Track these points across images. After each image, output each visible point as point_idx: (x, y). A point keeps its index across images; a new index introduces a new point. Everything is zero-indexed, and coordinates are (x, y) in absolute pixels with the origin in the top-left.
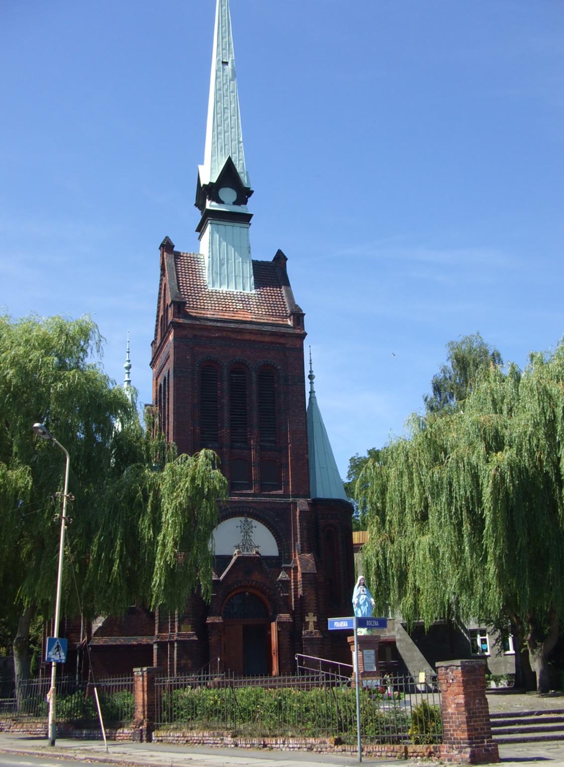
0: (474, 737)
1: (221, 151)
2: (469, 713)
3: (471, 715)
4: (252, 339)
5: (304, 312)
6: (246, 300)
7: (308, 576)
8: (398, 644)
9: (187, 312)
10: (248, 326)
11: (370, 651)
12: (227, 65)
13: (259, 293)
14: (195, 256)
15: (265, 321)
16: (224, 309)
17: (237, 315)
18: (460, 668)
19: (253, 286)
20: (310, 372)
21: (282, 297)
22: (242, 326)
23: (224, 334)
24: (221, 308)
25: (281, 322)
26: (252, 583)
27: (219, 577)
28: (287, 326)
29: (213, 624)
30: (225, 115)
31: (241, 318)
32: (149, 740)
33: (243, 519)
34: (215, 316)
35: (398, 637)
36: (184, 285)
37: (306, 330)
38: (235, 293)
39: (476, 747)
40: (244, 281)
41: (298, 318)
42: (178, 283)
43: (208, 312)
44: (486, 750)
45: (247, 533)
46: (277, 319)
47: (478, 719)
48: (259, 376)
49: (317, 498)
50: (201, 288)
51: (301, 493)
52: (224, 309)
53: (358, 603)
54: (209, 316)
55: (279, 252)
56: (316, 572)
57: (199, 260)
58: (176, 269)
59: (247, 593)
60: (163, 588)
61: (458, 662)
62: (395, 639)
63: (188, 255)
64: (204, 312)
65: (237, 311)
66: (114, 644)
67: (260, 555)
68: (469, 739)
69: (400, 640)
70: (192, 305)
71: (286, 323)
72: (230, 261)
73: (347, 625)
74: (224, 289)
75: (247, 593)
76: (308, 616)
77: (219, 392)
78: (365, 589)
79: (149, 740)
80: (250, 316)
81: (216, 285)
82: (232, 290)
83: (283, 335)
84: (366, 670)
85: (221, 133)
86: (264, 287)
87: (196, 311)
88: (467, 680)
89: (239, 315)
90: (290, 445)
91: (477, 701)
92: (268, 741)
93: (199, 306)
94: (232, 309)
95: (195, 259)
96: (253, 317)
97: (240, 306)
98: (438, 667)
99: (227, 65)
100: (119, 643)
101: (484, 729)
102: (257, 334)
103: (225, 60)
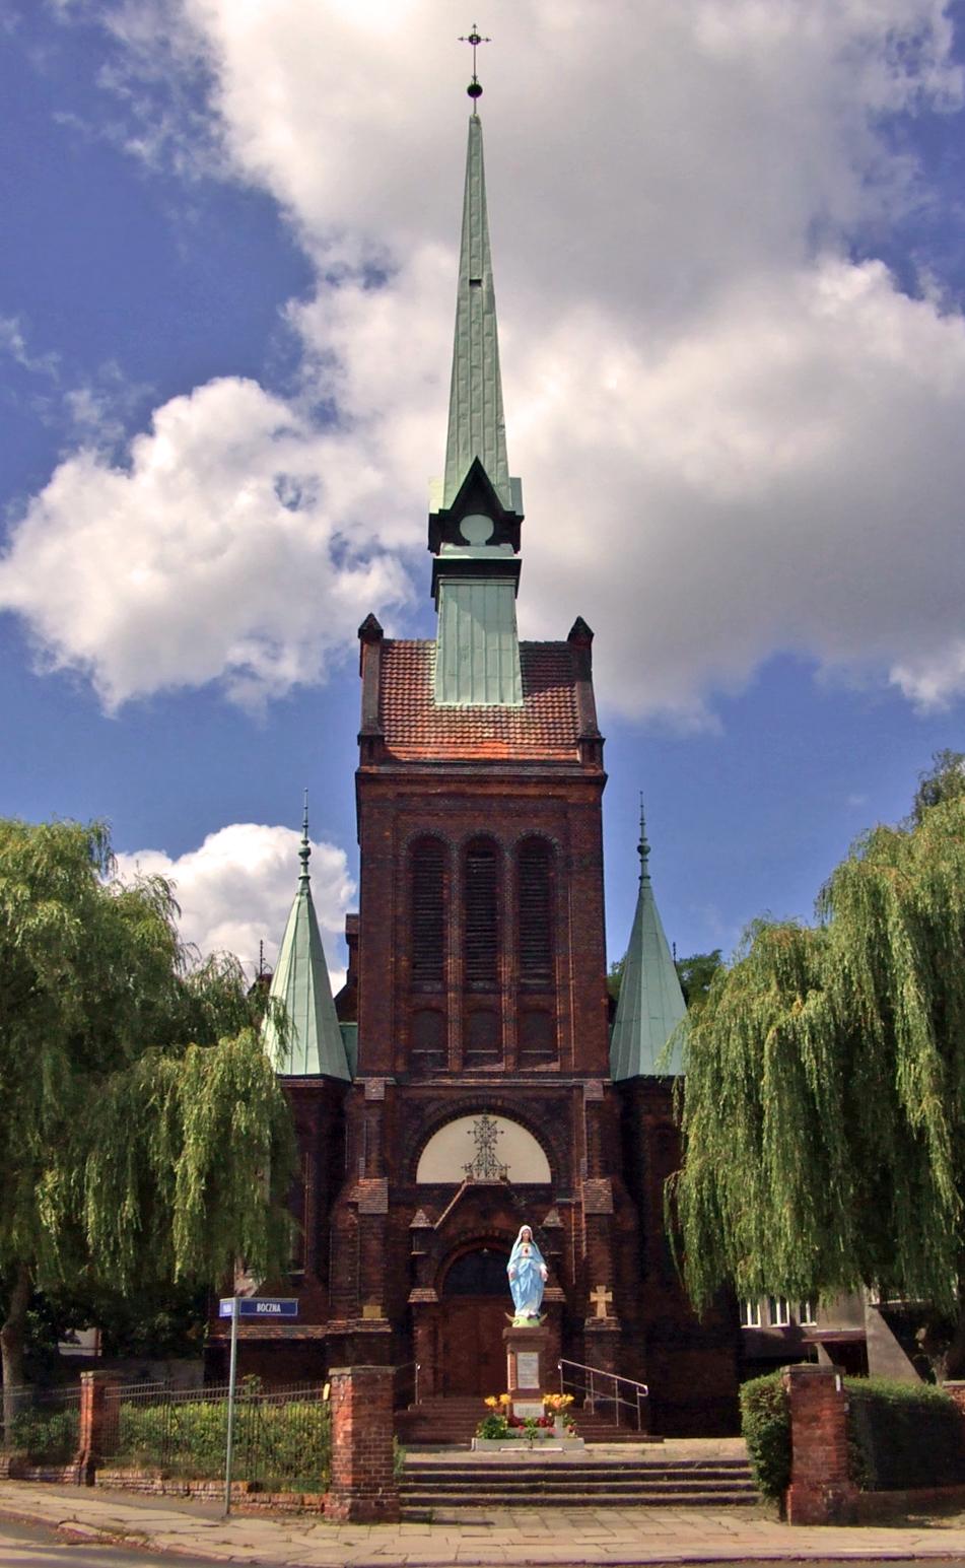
0: (362, 1483)
1: (464, 449)
2: (358, 1447)
3: (362, 1450)
4: (504, 793)
5: (603, 736)
6: (504, 719)
7: (597, 1219)
8: (869, 1345)
9: (390, 752)
10: (496, 770)
11: (530, 1354)
12: (480, 285)
13: (530, 704)
14: (421, 646)
15: (535, 757)
16: (459, 741)
17: (481, 750)
18: (350, 1378)
19: (521, 693)
20: (641, 840)
21: (574, 708)
22: (485, 771)
23: (453, 787)
24: (453, 740)
25: (563, 757)
26: (493, 1232)
27: (433, 1221)
28: (572, 763)
29: (420, 1305)
30: (474, 378)
31: (487, 756)
32: (91, 1483)
33: (479, 1118)
34: (441, 756)
35: (870, 1332)
36: (393, 701)
37: (606, 769)
38: (484, 709)
39: (361, 1498)
40: (503, 683)
41: (592, 746)
42: (381, 698)
43: (430, 750)
44: (377, 1504)
45: (486, 1142)
46: (557, 751)
47: (372, 1456)
48: (520, 857)
49: (638, 1079)
50: (422, 705)
51: (592, 1069)
52: (459, 741)
53: (516, 1271)
54: (429, 756)
55: (580, 622)
56: (611, 1211)
57: (427, 652)
58: (381, 673)
59: (485, 1250)
60: (57, 1251)
61: (348, 1370)
62: (865, 1337)
63: (408, 645)
64: (420, 750)
65: (482, 743)
66: (265, 1337)
67: (509, 1182)
68: (353, 1485)
69: (874, 1338)
70: (400, 739)
71: (573, 756)
72: (477, 651)
73: (279, 1310)
74: (466, 703)
75: (485, 1250)
76: (596, 1292)
77: (445, 892)
78: (529, 1249)
79: (91, 1483)
80: (506, 751)
81: (449, 695)
82: (479, 704)
83: (562, 781)
84: (520, 1386)
85: (464, 415)
86: (540, 692)
87: (406, 749)
88: (360, 1397)
89: (486, 750)
90: (572, 982)
91: (374, 1429)
92: (194, 1485)
93: (413, 740)
94: (473, 740)
95: (420, 652)
96: (512, 750)
97: (489, 733)
98: (332, 1376)
99: (480, 285)
100: (273, 1336)
101: (380, 1472)
102: (513, 782)
103: (475, 278)
